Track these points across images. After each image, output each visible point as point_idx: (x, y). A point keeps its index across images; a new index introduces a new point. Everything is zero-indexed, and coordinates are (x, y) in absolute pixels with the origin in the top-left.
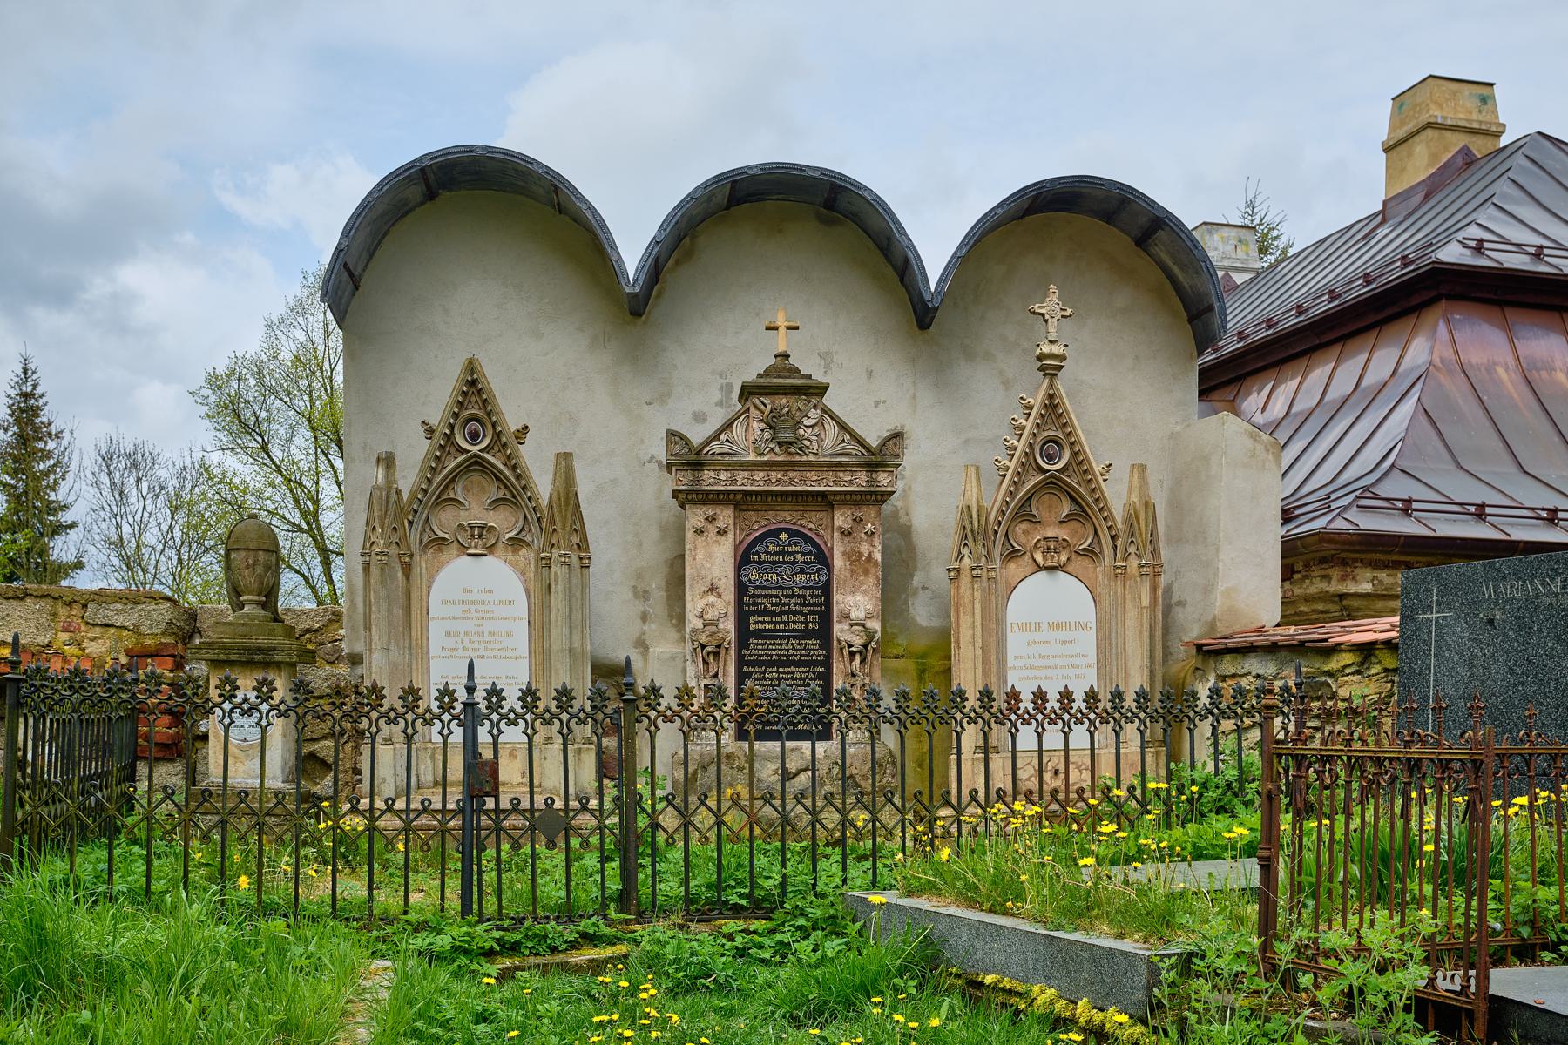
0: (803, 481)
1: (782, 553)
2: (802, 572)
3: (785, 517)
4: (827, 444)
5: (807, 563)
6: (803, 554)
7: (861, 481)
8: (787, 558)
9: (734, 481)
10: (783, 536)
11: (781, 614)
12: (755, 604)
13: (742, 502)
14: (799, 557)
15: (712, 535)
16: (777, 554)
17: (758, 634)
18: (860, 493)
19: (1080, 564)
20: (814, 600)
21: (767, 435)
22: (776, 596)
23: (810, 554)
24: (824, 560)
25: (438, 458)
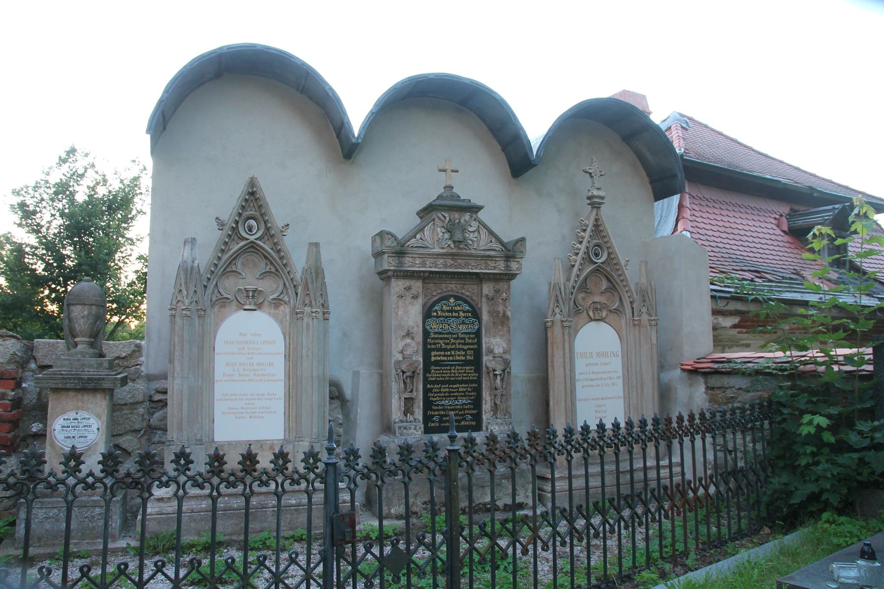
0: (467, 265)
1: (451, 311)
2: (463, 323)
3: (453, 287)
4: (482, 243)
5: (467, 317)
6: (464, 312)
7: (499, 267)
8: (454, 314)
9: (424, 265)
10: (452, 300)
11: (451, 350)
12: (434, 344)
13: (427, 277)
14: (461, 314)
15: (409, 300)
16: (448, 311)
17: (437, 363)
18: (500, 274)
19: (612, 317)
20: (471, 341)
21: (447, 236)
22: (448, 339)
23: (468, 311)
24: (476, 314)
25: (226, 243)
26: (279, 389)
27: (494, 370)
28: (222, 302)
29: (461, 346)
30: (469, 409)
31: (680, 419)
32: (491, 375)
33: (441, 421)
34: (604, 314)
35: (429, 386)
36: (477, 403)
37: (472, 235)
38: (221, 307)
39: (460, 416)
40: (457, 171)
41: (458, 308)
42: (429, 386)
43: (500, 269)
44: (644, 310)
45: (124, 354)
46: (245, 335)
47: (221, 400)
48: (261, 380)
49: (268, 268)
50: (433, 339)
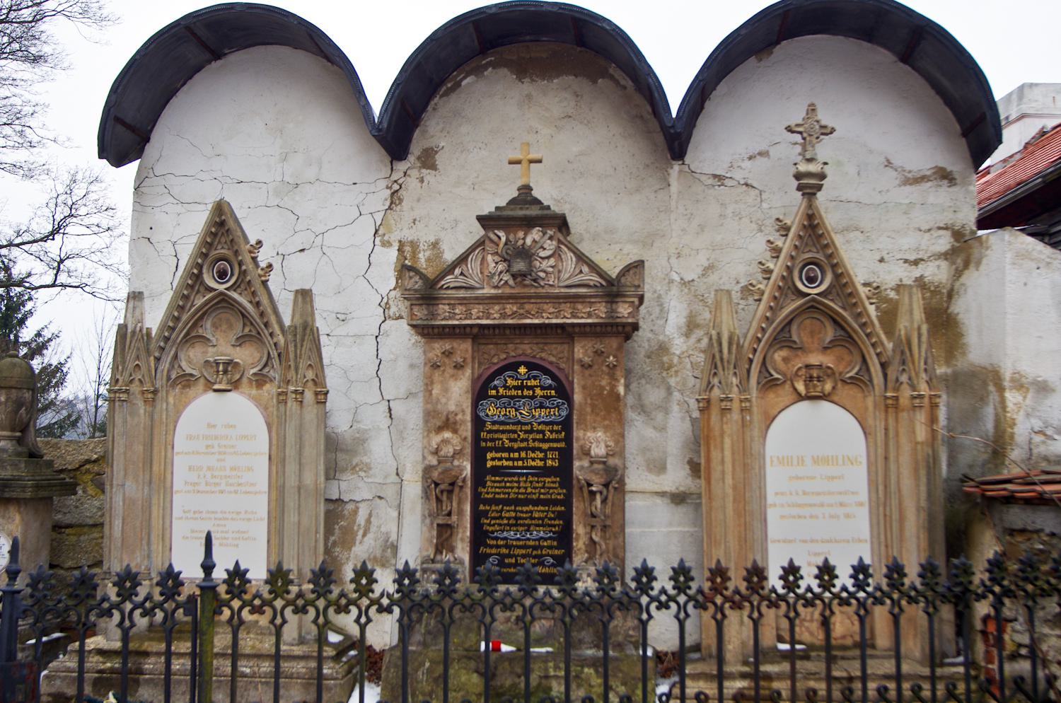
0: (539, 313)
1: (521, 388)
2: (541, 406)
3: (527, 349)
4: (565, 275)
5: (547, 397)
6: (543, 388)
7: (599, 313)
8: (526, 392)
10: (522, 370)
11: (519, 450)
12: (493, 440)
13: (479, 335)
14: (538, 391)
15: (450, 371)
16: (516, 388)
17: (496, 471)
19: (845, 392)
20: (554, 436)
22: (515, 432)
23: (550, 388)
24: (564, 393)
25: (186, 298)
26: (260, 505)
27: (590, 485)
28: (186, 381)
29: (537, 444)
30: (550, 547)
31: (791, 572)
32: (586, 494)
33: (501, 564)
34: (828, 387)
35: (482, 507)
36: (565, 537)
37: (545, 263)
38: (184, 387)
39: (535, 557)
40: (540, 161)
41: (532, 383)
42: (482, 507)
43: (598, 317)
44: (904, 378)
45: (95, 456)
46: (214, 426)
47: (181, 518)
48: (236, 492)
49: (247, 330)
50: (490, 432)
